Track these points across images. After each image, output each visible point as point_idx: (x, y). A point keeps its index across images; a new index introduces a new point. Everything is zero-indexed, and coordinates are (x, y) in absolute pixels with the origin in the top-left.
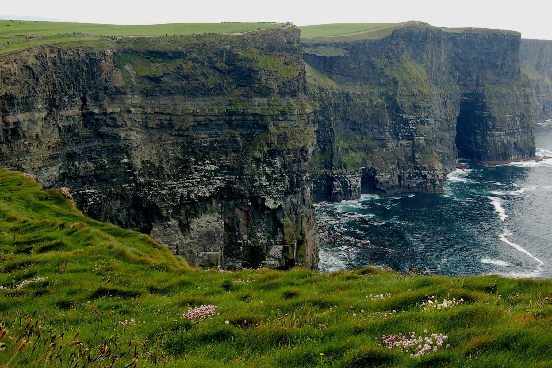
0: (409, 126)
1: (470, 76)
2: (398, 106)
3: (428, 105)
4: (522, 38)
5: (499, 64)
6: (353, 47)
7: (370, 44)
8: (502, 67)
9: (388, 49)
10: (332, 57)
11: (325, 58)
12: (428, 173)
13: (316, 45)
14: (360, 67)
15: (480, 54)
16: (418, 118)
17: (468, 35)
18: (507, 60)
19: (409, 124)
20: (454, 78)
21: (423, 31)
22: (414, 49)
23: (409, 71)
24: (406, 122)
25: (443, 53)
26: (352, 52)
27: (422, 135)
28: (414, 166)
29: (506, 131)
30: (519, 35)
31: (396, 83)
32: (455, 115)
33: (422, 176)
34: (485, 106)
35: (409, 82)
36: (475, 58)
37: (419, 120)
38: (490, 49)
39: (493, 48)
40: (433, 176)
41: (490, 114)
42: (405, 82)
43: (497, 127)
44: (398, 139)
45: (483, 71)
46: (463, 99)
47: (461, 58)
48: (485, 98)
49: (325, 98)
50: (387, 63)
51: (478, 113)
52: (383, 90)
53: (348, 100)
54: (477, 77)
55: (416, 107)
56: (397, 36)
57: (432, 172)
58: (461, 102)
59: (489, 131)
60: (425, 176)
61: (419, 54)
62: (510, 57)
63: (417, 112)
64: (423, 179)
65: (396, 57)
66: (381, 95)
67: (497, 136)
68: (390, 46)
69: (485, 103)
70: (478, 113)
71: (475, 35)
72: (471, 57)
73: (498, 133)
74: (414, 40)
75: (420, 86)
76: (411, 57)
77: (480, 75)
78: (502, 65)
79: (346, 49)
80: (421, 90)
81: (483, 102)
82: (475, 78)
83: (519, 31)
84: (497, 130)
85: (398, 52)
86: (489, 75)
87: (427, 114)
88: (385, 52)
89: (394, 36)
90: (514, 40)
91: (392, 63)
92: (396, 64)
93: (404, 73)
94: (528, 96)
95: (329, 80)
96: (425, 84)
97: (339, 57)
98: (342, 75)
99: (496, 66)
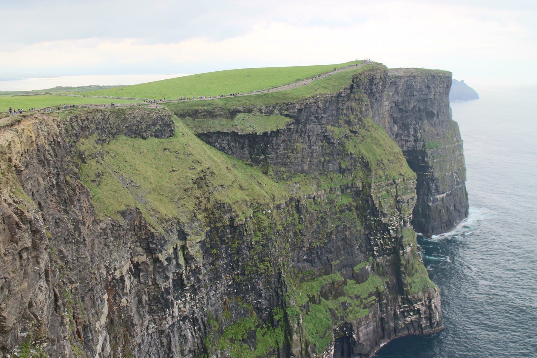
0: (389, 233)
1: (408, 129)
2: (374, 205)
4: (453, 78)
5: (435, 112)
6: (300, 111)
7: (325, 102)
8: (438, 114)
9: (347, 108)
10: (265, 134)
11: (252, 138)
12: (422, 304)
13: (233, 113)
14: (310, 146)
17: (408, 79)
19: (389, 231)
23: (382, 142)
24: (385, 229)
26: (298, 122)
31: (366, 165)
33: (414, 311)
34: (428, 167)
35: (386, 162)
36: (415, 107)
37: (402, 222)
38: (427, 94)
41: (433, 176)
42: (380, 163)
43: (440, 189)
44: (374, 256)
48: (427, 156)
49: (266, 224)
50: (348, 132)
52: (348, 179)
53: (298, 210)
55: (398, 202)
56: (358, 86)
59: (431, 195)
60: (419, 310)
63: (399, 210)
64: (414, 314)
65: (360, 120)
66: (344, 189)
68: (349, 104)
69: (427, 162)
73: (441, 196)
77: (418, 128)
78: (437, 112)
79: (286, 116)
81: (424, 161)
82: (412, 132)
83: (450, 71)
85: (361, 112)
86: (426, 125)
88: (344, 114)
89: (355, 85)
91: (355, 132)
92: (362, 132)
93: (375, 147)
95: (265, 179)
97: (277, 133)
98: (285, 165)
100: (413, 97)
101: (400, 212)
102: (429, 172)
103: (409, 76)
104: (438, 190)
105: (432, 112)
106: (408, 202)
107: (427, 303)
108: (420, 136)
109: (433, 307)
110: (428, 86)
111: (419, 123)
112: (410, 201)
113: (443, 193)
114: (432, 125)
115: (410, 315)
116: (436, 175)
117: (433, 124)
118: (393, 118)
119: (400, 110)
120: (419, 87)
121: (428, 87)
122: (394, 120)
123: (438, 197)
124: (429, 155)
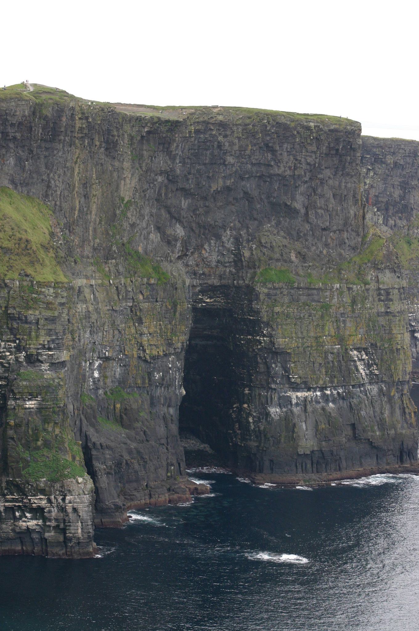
3: (49, 314)
4: (364, 133)
8: (307, 214)
12: (49, 501)
15: (242, 179)
16: (19, 349)
17: (200, 127)
18: (322, 196)
20: (169, 243)
21: (48, 112)
22: (19, 160)
25: (127, 174)
27: (32, 396)
28: (8, 482)
29: (322, 389)
30: (355, 127)
32: (170, 344)
38: (269, 165)
39: (278, 162)
40: (63, 509)
41: (273, 343)
43: (295, 378)
45: (253, 225)
46: (201, 301)
47: (183, 189)
48: (257, 298)
51: (243, 339)
54: (237, 241)
57: (60, 498)
58: (195, 309)
61: (38, 173)
62: (332, 188)
67: (297, 404)
69: (258, 312)
70: (243, 339)
71: (222, 125)
72: (214, 187)
74: (18, 135)
75: (26, 259)
76: (13, 182)
77: (245, 236)
78: (307, 208)
80: (30, 271)
82: (230, 245)
84: (296, 388)
86: (272, 234)
87: (44, 339)
90: (337, 140)
94: (388, 294)
96: (42, 254)
99: (291, 212)
100: (222, 168)
101: (15, 335)
102: (264, 336)
103: (206, 123)
104: (289, 379)
105: (286, 205)
106: (37, 323)
107: (60, 500)
108: (247, 254)
109: (69, 508)
110: (267, 146)
111: (248, 228)
112: (42, 322)
113: (309, 389)
114: (289, 234)
115: (26, 517)
116: (281, 342)
117: (294, 233)
118: (168, 209)
119: (186, 193)
120: (236, 147)
121: (269, 148)
122: (169, 212)
123: (296, 396)
124: (262, 297)
